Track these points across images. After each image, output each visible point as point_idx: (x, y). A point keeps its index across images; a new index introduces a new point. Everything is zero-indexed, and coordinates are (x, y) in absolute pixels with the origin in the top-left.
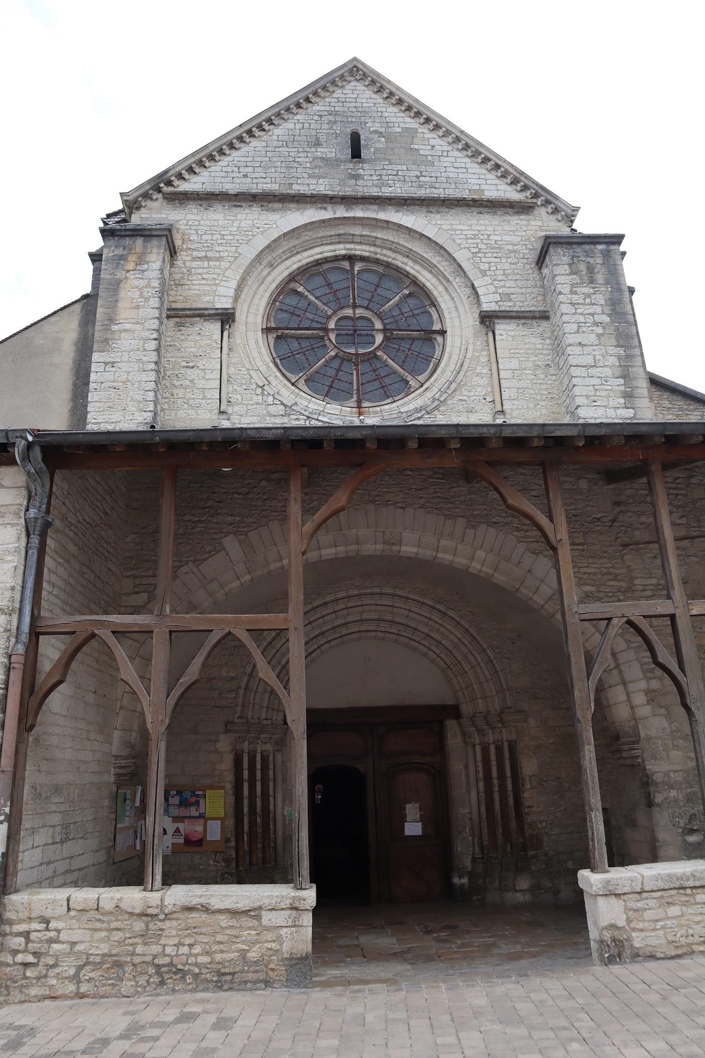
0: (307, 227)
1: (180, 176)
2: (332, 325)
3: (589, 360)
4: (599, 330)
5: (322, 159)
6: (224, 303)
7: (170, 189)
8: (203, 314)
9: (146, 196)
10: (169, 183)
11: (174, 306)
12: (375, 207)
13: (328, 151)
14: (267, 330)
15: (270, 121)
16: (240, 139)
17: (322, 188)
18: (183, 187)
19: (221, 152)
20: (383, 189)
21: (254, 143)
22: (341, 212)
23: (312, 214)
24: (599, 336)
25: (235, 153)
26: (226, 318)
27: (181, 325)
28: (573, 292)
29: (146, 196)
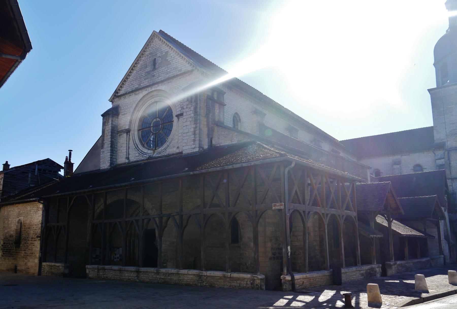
0: (144, 97)
1: (119, 90)
2: (152, 125)
3: (187, 131)
4: (191, 119)
5: (147, 72)
6: (127, 128)
7: (119, 94)
8: (122, 131)
9: (114, 98)
10: (117, 93)
11: (119, 130)
12: (156, 86)
13: (149, 69)
14: (139, 130)
15: (136, 63)
16: (130, 72)
17: (146, 83)
18: (121, 92)
19: (127, 78)
20: (159, 78)
21: (135, 72)
22: (149, 90)
23: (144, 92)
24: (190, 121)
25: (130, 77)
26: (128, 131)
27: (120, 135)
28: (187, 108)
29: (114, 98)
